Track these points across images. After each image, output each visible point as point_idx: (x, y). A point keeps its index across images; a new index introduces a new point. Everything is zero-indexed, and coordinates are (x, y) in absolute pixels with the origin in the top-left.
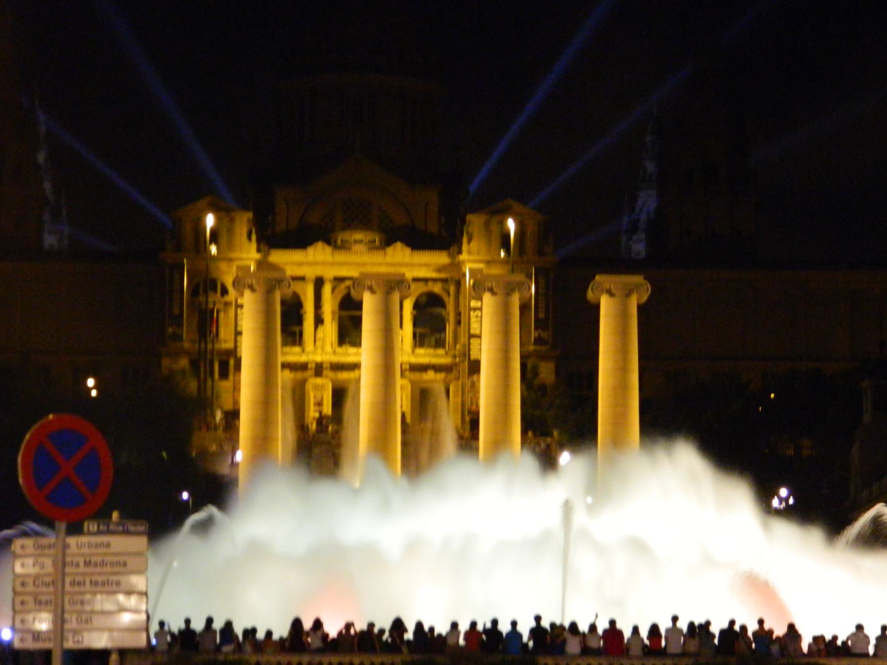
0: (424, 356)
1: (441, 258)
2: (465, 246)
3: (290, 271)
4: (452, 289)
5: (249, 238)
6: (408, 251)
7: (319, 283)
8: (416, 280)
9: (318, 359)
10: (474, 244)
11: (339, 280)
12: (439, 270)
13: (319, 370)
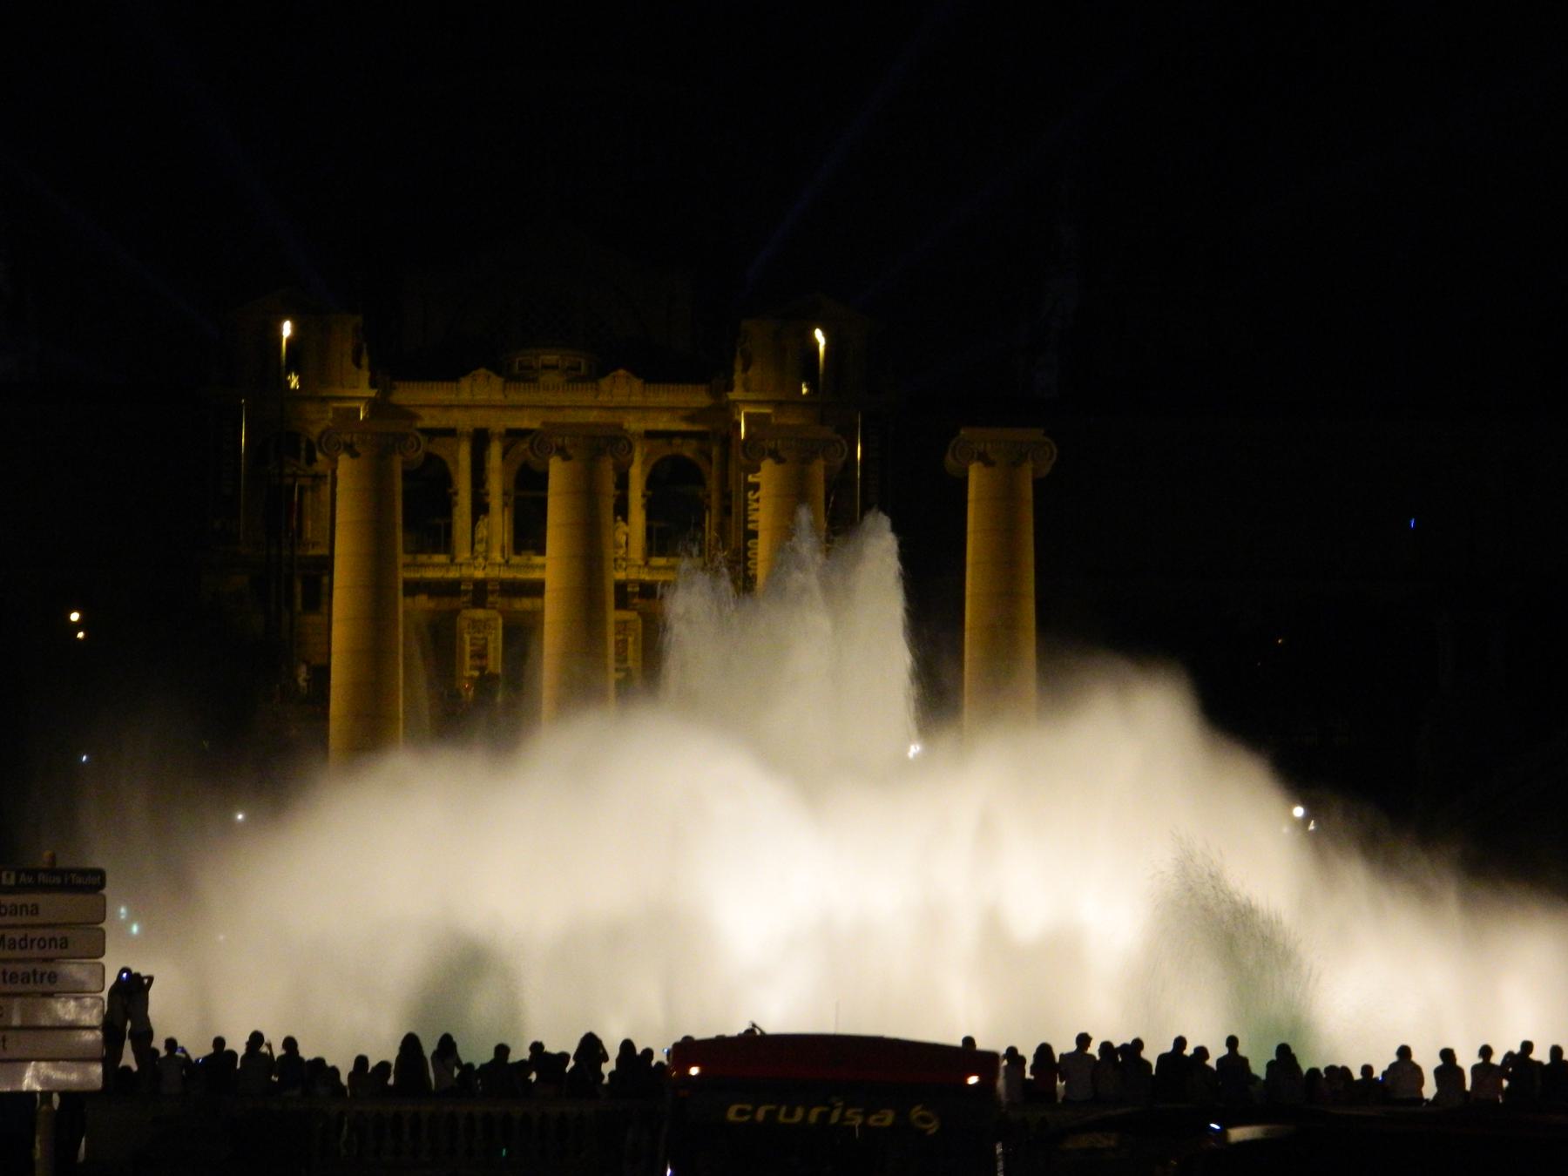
1: (698, 398)
2: (738, 377)
3: (429, 420)
5: (358, 365)
6: (637, 383)
7: (480, 440)
8: (650, 435)
12: (691, 418)
13: (480, 592)
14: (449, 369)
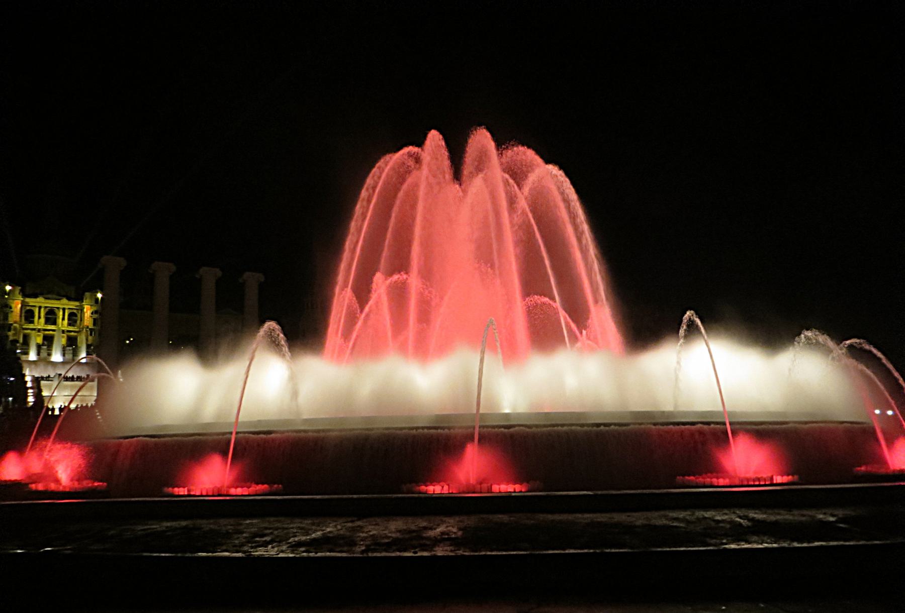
0: (71, 328)
1: (77, 303)
2: (84, 301)
4: (80, 312)
7: (40, 308)
8: (69, 309)
9: (39, 327)
10: (87, 301)
11: (46, 307)
12: (76, 307)
13: (39, 330)
14: (35, 296)
